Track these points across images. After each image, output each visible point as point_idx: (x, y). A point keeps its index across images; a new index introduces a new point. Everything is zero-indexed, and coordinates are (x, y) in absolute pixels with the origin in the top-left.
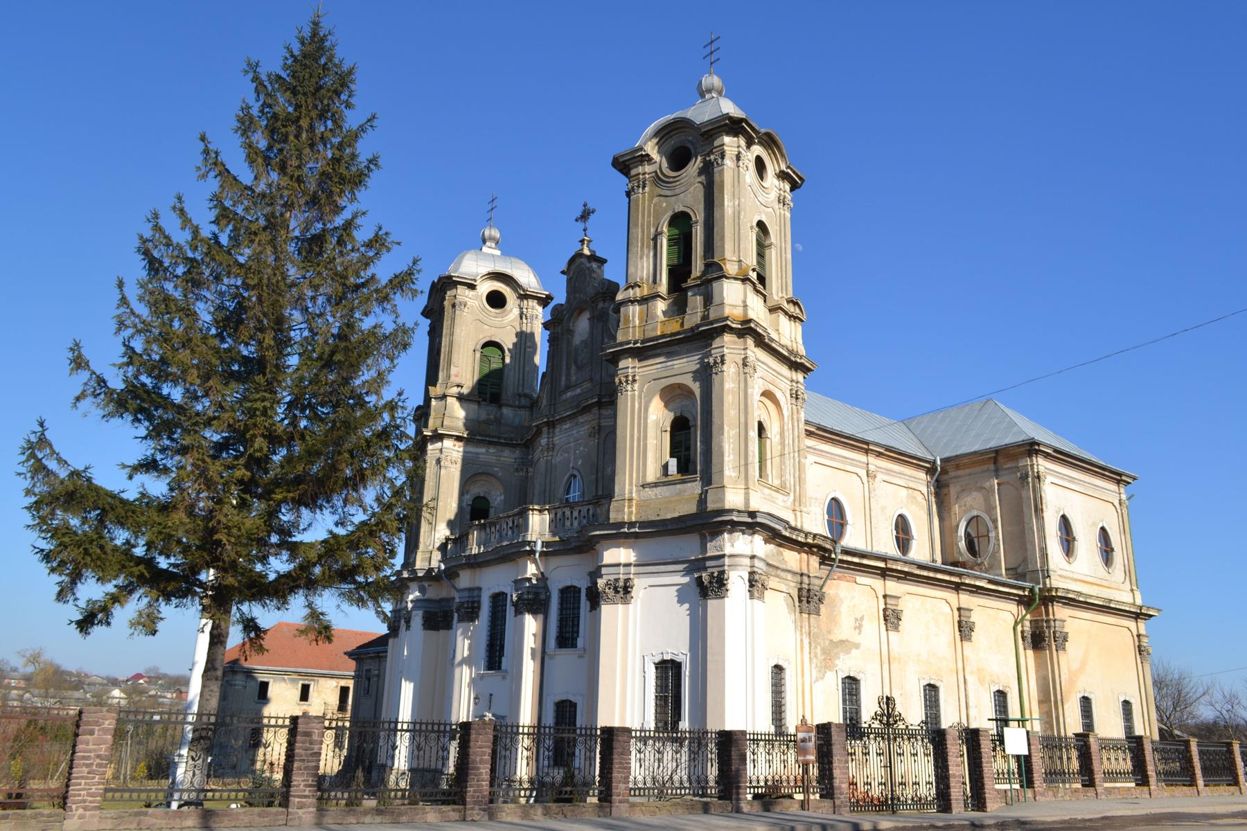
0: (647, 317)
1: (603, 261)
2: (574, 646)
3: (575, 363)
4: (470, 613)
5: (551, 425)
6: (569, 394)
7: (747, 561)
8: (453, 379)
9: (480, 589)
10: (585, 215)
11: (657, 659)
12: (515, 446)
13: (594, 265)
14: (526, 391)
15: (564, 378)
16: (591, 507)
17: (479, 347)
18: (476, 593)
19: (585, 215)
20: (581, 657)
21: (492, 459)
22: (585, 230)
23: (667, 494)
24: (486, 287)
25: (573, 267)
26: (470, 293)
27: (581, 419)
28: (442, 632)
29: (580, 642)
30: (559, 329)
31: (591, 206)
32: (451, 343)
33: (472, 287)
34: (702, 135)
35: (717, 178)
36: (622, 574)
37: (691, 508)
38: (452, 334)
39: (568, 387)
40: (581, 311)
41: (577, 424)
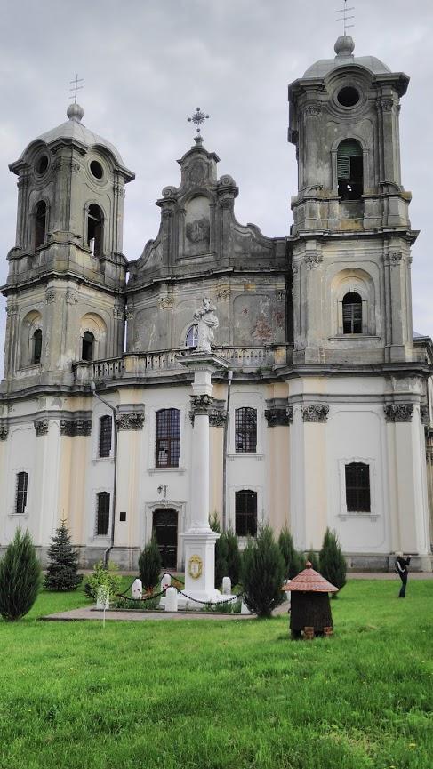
0: (328, 214)
1: (217, 160)
2: (254, 450)
3: (189, 236)
4: (137, 423)
5: (171, 283)
6: (188, 262)
7: (419, 398)
8: (72, 230)
9: (144, 405)
10: (198, 119)
11: (348, 463)
12: (113, 295)
13: (213, 161)
14: (119, 252)
15: (181, 247)
16: (262, 350)
17: (87, 207)
18: (139, 408)
19: (198, 119)
20: (260, 458)
21: (99, 303)
22: (199, 130)
23: (352, 347)
24: (91, 157)
25: (189, 159)
26: (81, 159)
27: (205, 283)
28: (79, 439)
29: (258, 447)
30: (172, 207)
31: (204, 111)
32: (69, 200)
33: (83, 153)
34: (373, 84)
35: (386, 120)
36: (319, 404)
37: (377, 359)
38: (69, 191)
39: (187, 257)
40: (198, 195)
41: (199, 285)
